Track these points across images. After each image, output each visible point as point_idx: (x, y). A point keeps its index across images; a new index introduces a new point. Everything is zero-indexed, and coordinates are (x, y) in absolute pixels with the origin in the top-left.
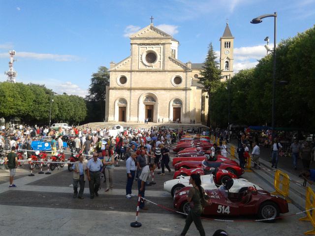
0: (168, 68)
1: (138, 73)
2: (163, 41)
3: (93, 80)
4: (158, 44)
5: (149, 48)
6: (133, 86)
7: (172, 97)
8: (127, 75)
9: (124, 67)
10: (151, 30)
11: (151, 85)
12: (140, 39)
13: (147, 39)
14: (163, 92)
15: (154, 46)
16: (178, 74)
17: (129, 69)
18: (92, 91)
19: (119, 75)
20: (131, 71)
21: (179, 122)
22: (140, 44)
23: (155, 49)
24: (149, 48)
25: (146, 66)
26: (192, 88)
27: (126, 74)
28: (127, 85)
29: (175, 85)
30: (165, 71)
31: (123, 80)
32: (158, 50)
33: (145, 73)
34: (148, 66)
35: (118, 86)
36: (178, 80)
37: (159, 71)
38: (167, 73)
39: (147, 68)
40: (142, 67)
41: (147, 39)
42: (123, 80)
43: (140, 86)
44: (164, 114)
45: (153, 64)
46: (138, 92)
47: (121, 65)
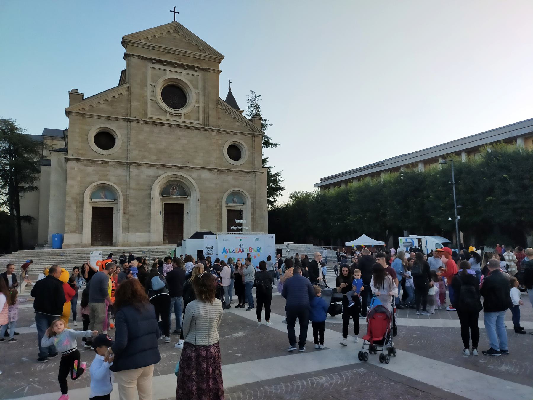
4: (192, 68)
5: (171, 74)
10: (175, 35)
13: (167, 51)
14: (206, 175)
15: (183, 71)
24: (171, 74)
25: (166, 112)
27: (112, 127)
32: (191, 81)
41: (167, 51)
47: (102, 102)
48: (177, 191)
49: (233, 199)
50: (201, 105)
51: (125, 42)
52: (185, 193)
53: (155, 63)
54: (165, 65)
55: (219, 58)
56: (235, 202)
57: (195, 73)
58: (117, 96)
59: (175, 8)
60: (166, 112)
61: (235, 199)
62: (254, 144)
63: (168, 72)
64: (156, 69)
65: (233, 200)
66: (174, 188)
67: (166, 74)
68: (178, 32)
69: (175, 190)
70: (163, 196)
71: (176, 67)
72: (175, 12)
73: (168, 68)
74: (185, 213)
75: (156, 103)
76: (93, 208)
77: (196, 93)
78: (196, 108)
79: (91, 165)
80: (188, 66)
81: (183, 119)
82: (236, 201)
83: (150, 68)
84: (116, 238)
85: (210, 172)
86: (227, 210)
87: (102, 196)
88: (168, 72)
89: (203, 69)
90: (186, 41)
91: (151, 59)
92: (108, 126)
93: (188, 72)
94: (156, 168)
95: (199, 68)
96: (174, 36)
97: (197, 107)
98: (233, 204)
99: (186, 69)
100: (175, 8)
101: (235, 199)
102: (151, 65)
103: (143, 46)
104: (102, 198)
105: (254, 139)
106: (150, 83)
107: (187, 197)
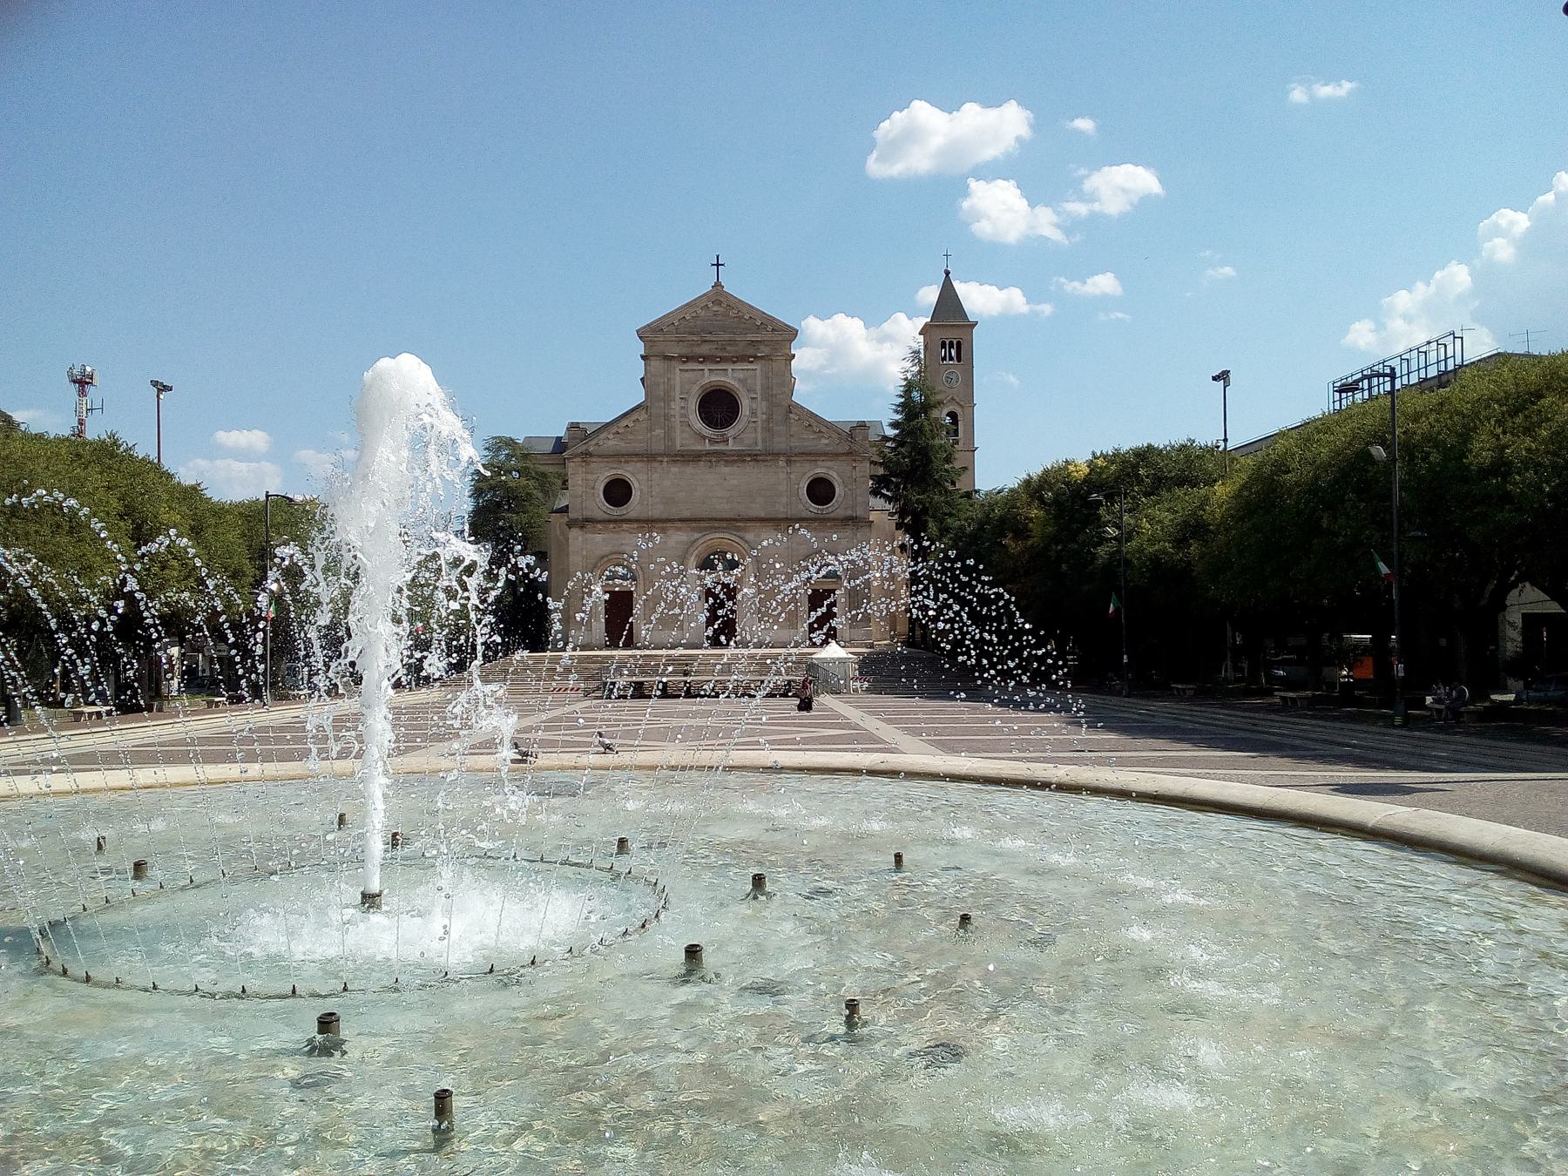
0: (780, 444)
1: (675, 469)
2: (764, 351)
5: (711, 376)
6: (657, 511)
8: (634, 475)
9: (623, 444)
11: (723, 508)
15: (730, 367)
16: (820, 471)
17: (639, 447)
19: (603, 475)
20: (650, 457)
22: (681, 357)
23: (730, 377)
25: (704, 438)
27: (627, 472)
28: (634, 507)
29: (814, 507)
30: (776, 455)
31: (618, 492)
35: (599, 515)
36: (821, 491)
39: (708, 447)
40: (682, 441)
42: (618, 492)
43: (686, 514)
45: (730, 432)
50: (761, 417)
51: (642, 333)
54: (701, 362)
57: (750, 367)
58: (631, 425)
63: (706, 372)
68: (720, 303)
72: (718, 265)
73: (706, 367)
77: (752, 398)
78: (752, 425)
81: (731, 446)
88: (706, 372)
93: (738, 366)
95: (755, 357)
99: (734, 362)
102: (679, 366)
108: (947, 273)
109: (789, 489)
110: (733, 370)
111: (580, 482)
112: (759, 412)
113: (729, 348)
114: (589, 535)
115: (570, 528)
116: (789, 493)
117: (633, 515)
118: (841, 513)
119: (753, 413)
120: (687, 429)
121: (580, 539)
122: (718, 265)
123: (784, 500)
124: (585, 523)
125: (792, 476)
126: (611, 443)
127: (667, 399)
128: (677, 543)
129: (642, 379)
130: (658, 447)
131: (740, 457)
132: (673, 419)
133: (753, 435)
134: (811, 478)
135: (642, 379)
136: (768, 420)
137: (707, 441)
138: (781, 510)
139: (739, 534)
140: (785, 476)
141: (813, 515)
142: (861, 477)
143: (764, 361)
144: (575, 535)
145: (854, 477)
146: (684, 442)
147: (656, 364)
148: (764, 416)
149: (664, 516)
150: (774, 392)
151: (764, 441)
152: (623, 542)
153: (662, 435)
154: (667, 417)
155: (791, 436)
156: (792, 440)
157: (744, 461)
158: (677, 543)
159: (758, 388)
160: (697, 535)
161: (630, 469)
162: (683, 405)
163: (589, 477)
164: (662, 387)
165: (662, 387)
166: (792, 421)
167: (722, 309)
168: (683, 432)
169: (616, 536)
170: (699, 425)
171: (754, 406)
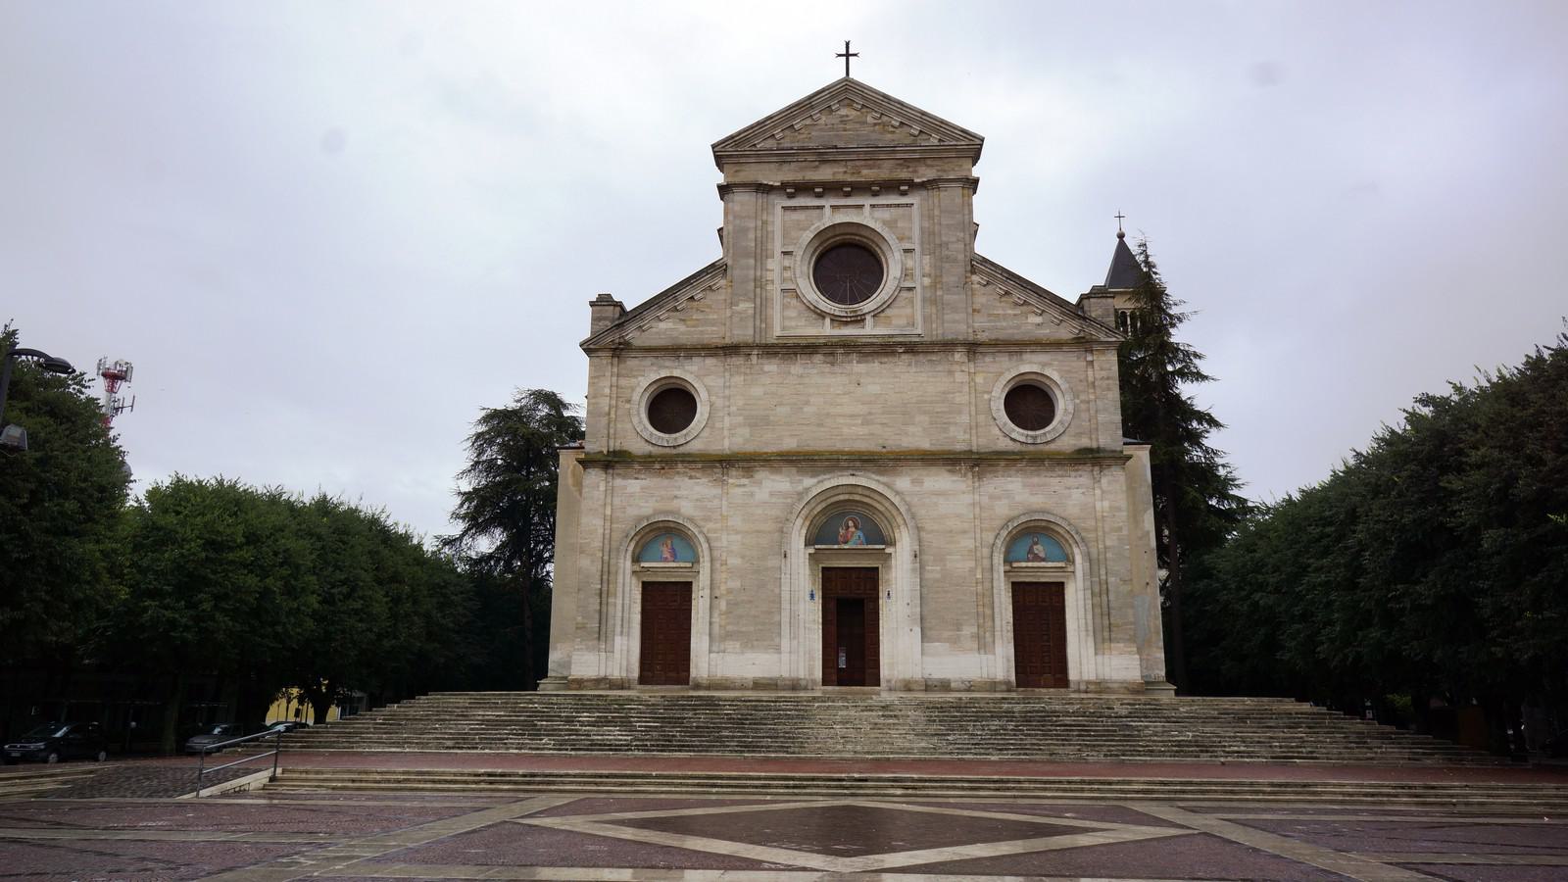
1: (772, 366)
3: (481, 441)
7: (1003, 510)
8: (701, 377)
9: (682, 328)
10: (844, 112)
11: (856, 437)
12: (783, 157)
14: (939, 480)
15: (867, 201)
16: (1030, 365)
18: (480, 510)
21: (1060, 678)
22: (784, 186)
23: (868, 214)
25: (822, 315)
26: (1128, 450)
27: (691, 373)
28: (698, 436)
29: (1019, 433)
30: (947, 346)
33: (818, 358)
34: (836, 320)
35: (637, 447)
37: (912, 348)
38: (959, 356)
39: (827, 330)
40: (788, 322)
43: (789, 444)
44: (958, 626)
46: (774, 487)
48: (859, 533)
49: (1031, 547)
50: (921, 282)
52: (879, 537)
53: (792, 193)
54: (819, 196)
55: (971, 146)
56: (1037, 558)
59: (847, 44)
60: (824, 318)
61: (1039, 549)
62: (1090, 373)
63: (828, 211)
64: (795, 209)
65: (1030, 551)
66: (851, 523)
67: (820, 218)
69: (853, 529)
70: (816, 547)
71: (848, 195)
72: (847, 55)
73: (828, 202)
74: (882, 595)
75: (797, 296)
76: (646, 586)
77: (906, 251)
79: (636, 476)
80: (852, 185)
81: (870, 329)
82: (1042, 555)
83: (779, 210)
84: (696, 667)
85: (949, 471)
86: (1013, 583)
87: (666, 555)
88: (828, 211)
89: (923, 186)
90: (876, 121)
91: (783, 188)
92: (676, 373)
94: (794, 470)
96: (843, 116)
97: (910, 289)
98: (1030, 564)
99: (875, 194)
100: (847, 44)
101: (1039, 549)
102: (780, 202)
103: (762, 157)
104: (666, 560)
105: (1089, 358)
106: (778, 247)
107: (883, 546)
108: (1121, 236)
109: (973, 401)
110: (872, 206)
111: (607, 391)
112: (917, 273)
113: (865, 172)
114: (618, 482)
115: (585, 468)
116: (973, 408)
117: (696, 447)
118: (1068, 443)
119: (907, 274)
120: (794, 302)
121: (602, 488)
122: (847, 55)
123: (965, 419)
124: (614, 461)
125: (979, 379)
126: (665, 329)
127: (761, 254)
128: (772, 494)
129: (720, 230)
130: (743, 333)
131: (885, 349)
132: (769, 287)
133: (909, 311)
134: (1007, 390)
135: (720, 230)
136: (934, 286)
137: (828, 321)
138: (959, 439)
139: (881, 479)
140: (965, 378)
141: (1017, 447)
142: (1102, 379)
143: (925, 193)
144: (595, 478)
145: (1091, 379)
146: (787, 323)
147: (743, 199)
148: (927, 281)
149: (750, 448)
150: (944, 239)
151: (926, 319)
152: (677, 493)
153: (751, 312)
154: (760, 283)
155: (974, 310)
156: (977, 317)
157: (893, 353)
158: (772, 494)
159: (916, 234)
160: (808, 482)
161: (695, 368)
162: (787, 263)
163: (623, 382)
164: (751, 236)
165: (751, 236)
166: (977, 286)
167: (854, 113)
168: (785, 307)
169: (666, 482)
170: (812, 294)
171: (910, 263)
